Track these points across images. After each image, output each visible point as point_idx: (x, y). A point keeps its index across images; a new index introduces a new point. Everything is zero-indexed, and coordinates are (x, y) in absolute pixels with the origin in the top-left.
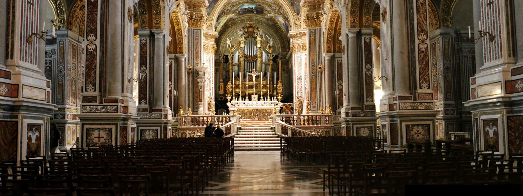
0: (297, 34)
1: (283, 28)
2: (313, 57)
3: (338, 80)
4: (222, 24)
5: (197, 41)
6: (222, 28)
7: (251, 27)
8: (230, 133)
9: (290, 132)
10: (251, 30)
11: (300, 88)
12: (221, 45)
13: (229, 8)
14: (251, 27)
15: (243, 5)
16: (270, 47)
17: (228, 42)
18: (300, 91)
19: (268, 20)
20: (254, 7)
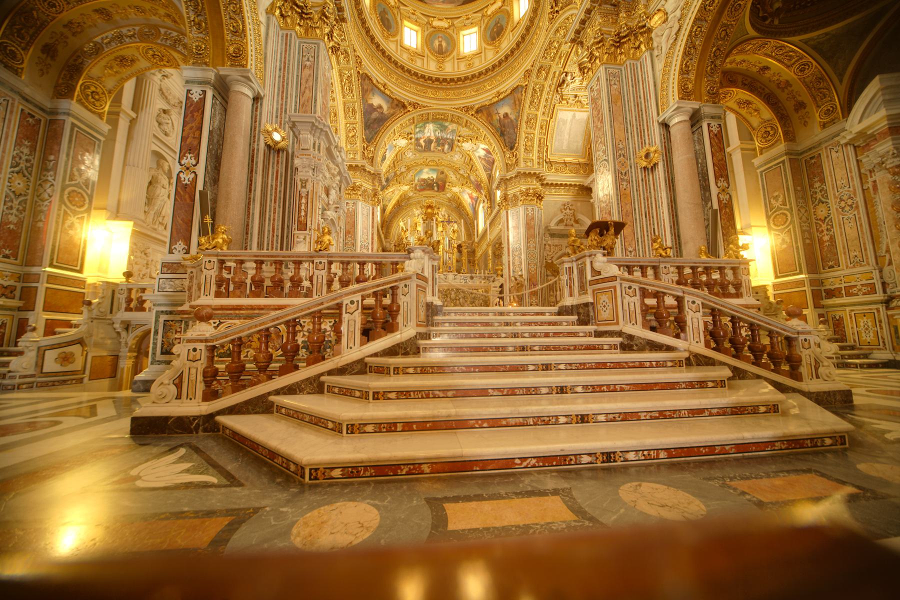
0: (511, 178)
1: (469, 210)
2: (620, 135)
3: (716, 178)
4: (393, 202)
5: (307, 72)
6: (393, 207)
7: (430, 207)
8: (389, 327)
9: (696, 319)
10: (429, 211)
11: (517, 263)
12: (394, 231)
13: (403, 170)
14: (430, 207)
15: (421, 171)
16: (454, 232)
17: (402, 224)
18: (517, 269)
19: (450, 200)
20: (435, 177)
